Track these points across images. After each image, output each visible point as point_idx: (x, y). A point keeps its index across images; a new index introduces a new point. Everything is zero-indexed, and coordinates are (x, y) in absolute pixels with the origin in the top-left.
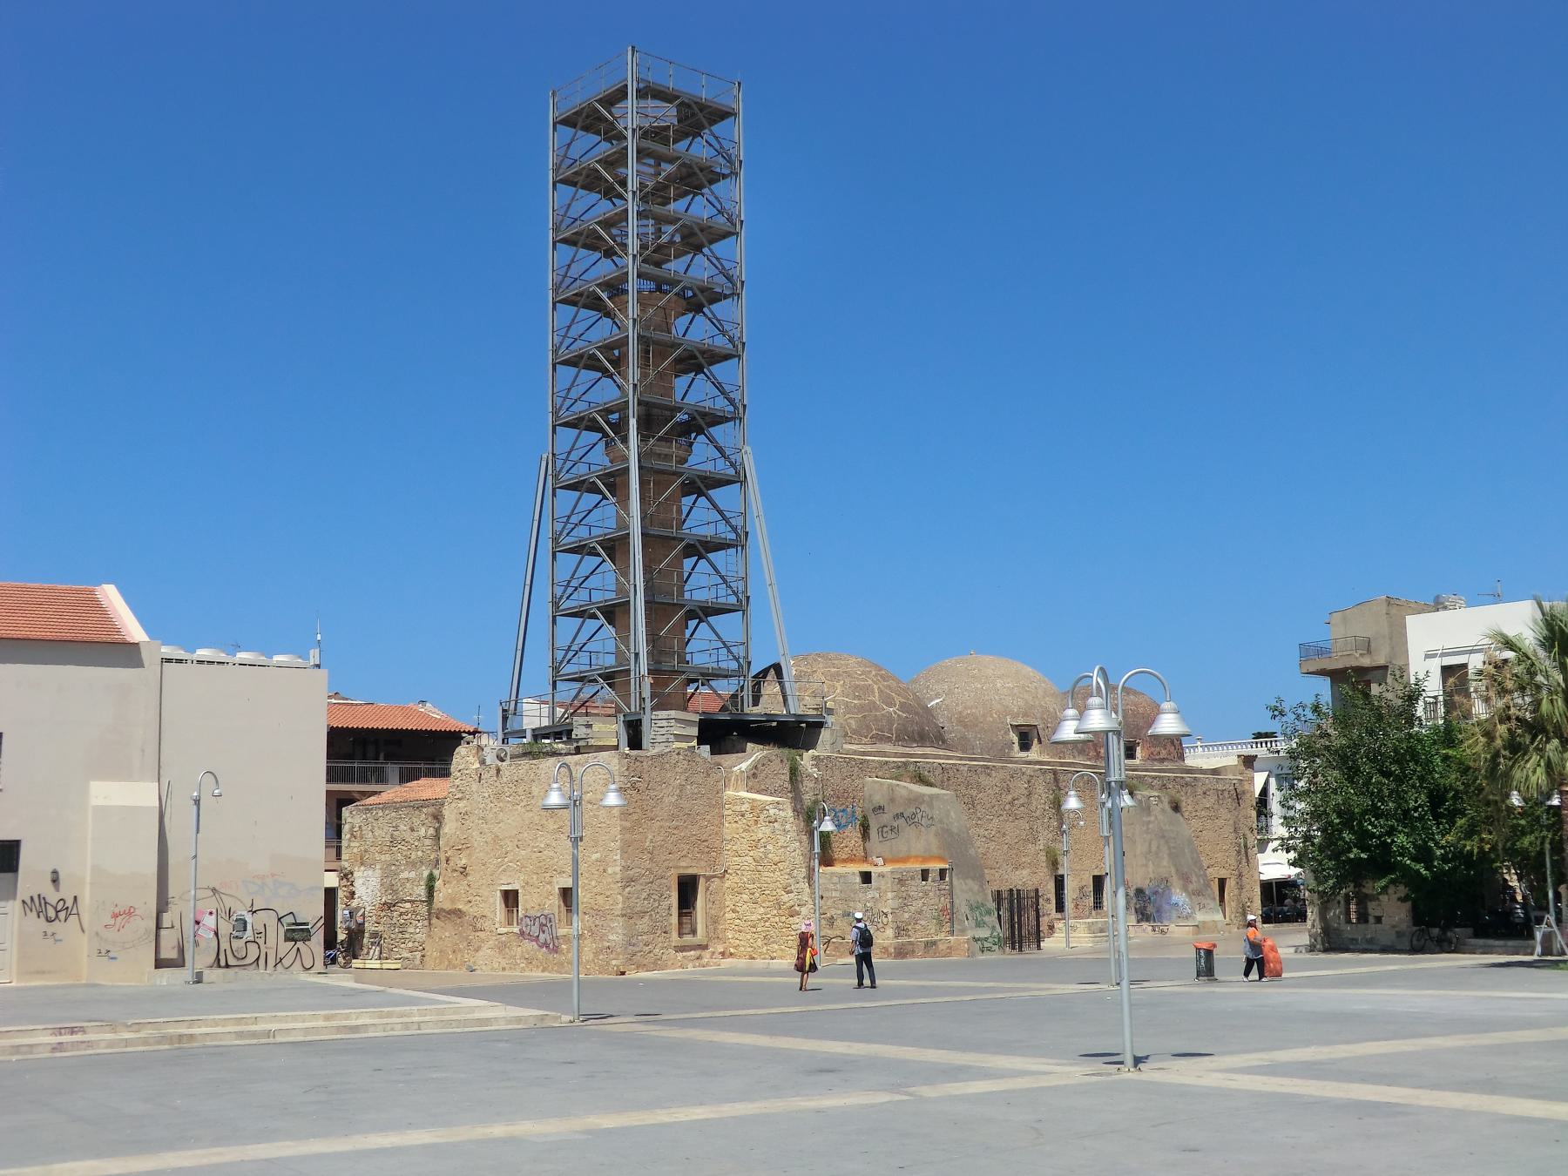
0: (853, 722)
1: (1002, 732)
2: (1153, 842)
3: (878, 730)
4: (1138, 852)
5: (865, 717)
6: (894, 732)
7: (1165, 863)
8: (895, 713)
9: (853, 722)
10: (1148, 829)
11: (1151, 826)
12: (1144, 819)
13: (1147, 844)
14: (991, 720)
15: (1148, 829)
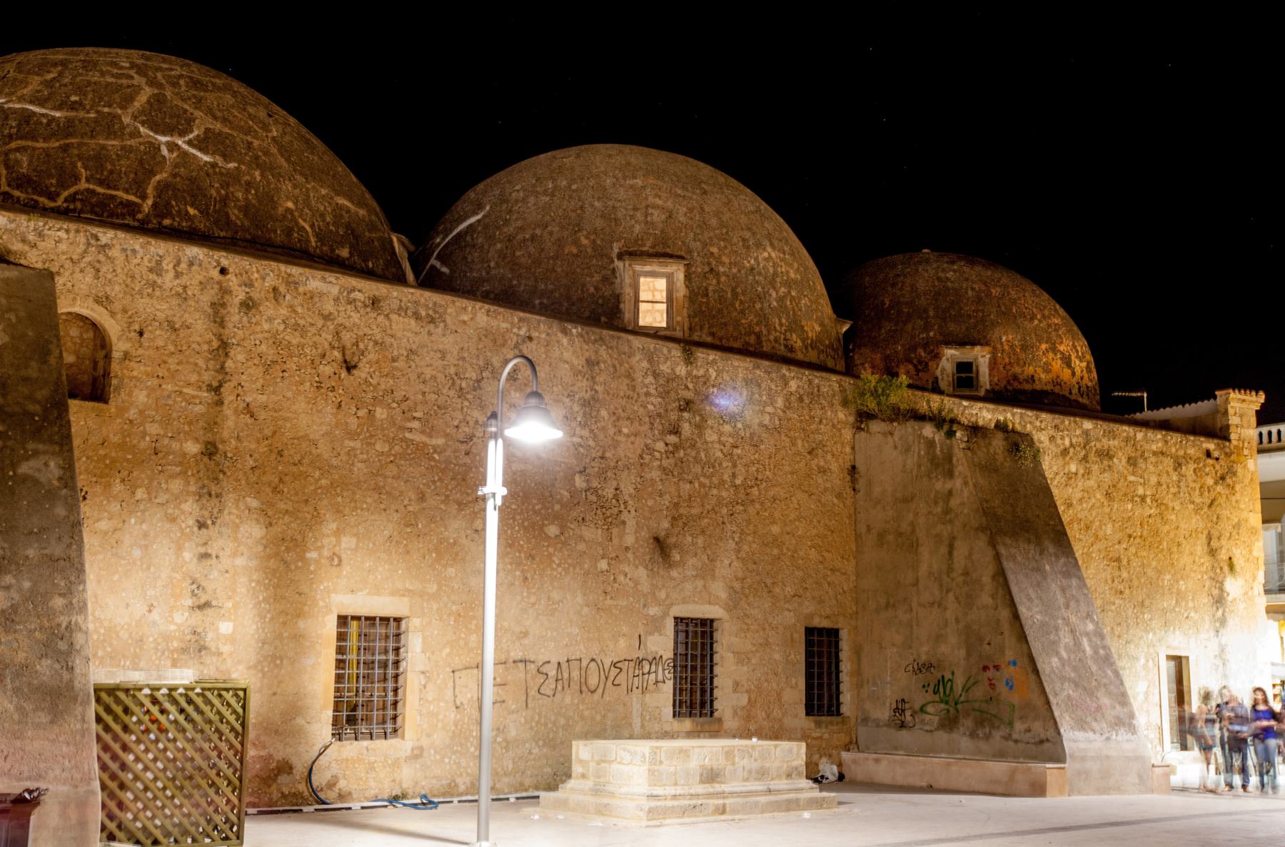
0: (24, 159)
1: (597, 277)
2: (958, 543)
3: (101, 183)
4: (923, 569)
5: (65, 148)
6: (150, 190)
7: (986, 599)
8: (172, 147)
9: (24, 159)
10: (947, 511)
11: (954, 502)
12: (939, 486)
13: (944, 550)
14: (575, 251)
15: (947, 511)
